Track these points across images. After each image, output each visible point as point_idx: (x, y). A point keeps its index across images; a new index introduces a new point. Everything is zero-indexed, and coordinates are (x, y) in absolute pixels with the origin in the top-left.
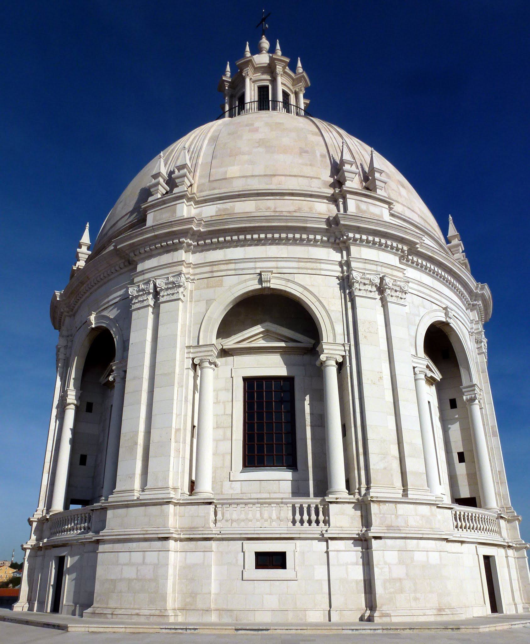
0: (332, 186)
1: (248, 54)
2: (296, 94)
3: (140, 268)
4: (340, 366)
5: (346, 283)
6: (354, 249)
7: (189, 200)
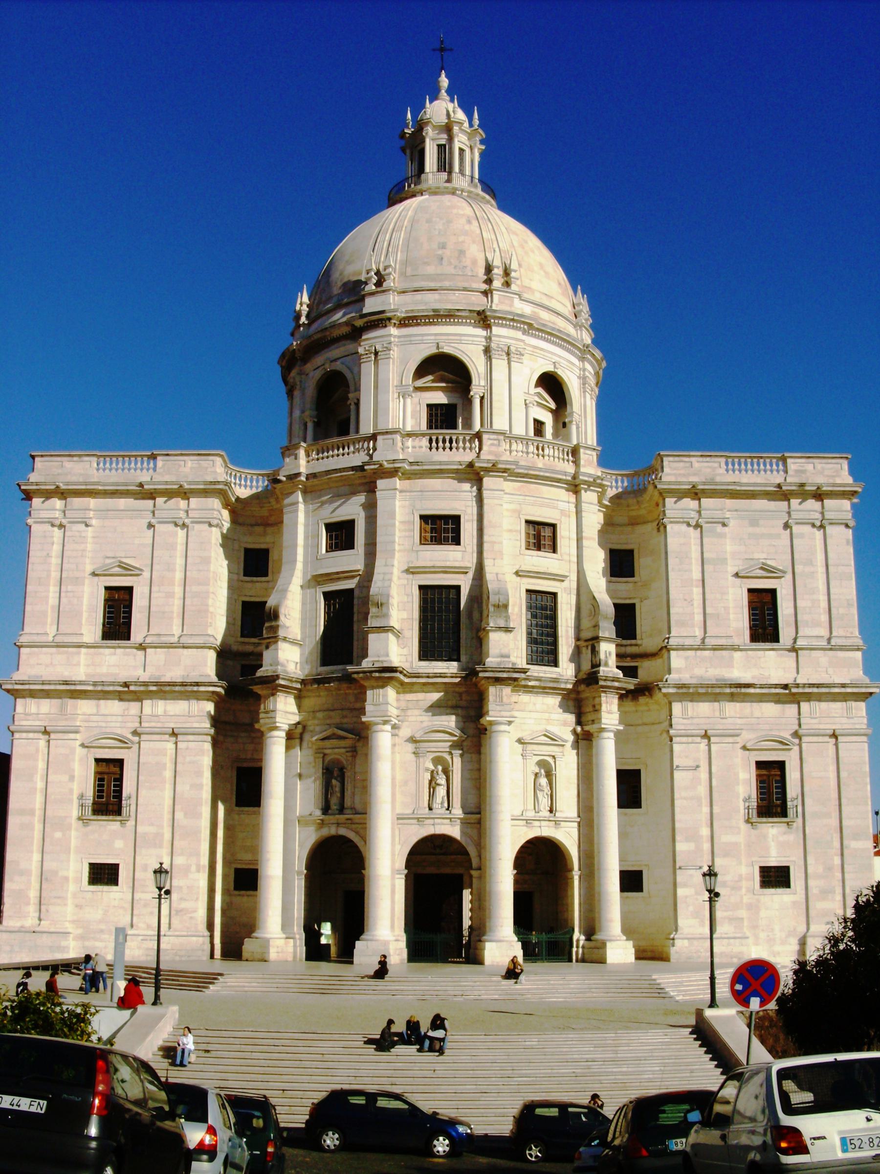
0: (486, 282)
2: (471, 148)
3: (364, 337)
4: (482, 398)
5: (487, 351)
6: (494, 328)
7: (394, 291)
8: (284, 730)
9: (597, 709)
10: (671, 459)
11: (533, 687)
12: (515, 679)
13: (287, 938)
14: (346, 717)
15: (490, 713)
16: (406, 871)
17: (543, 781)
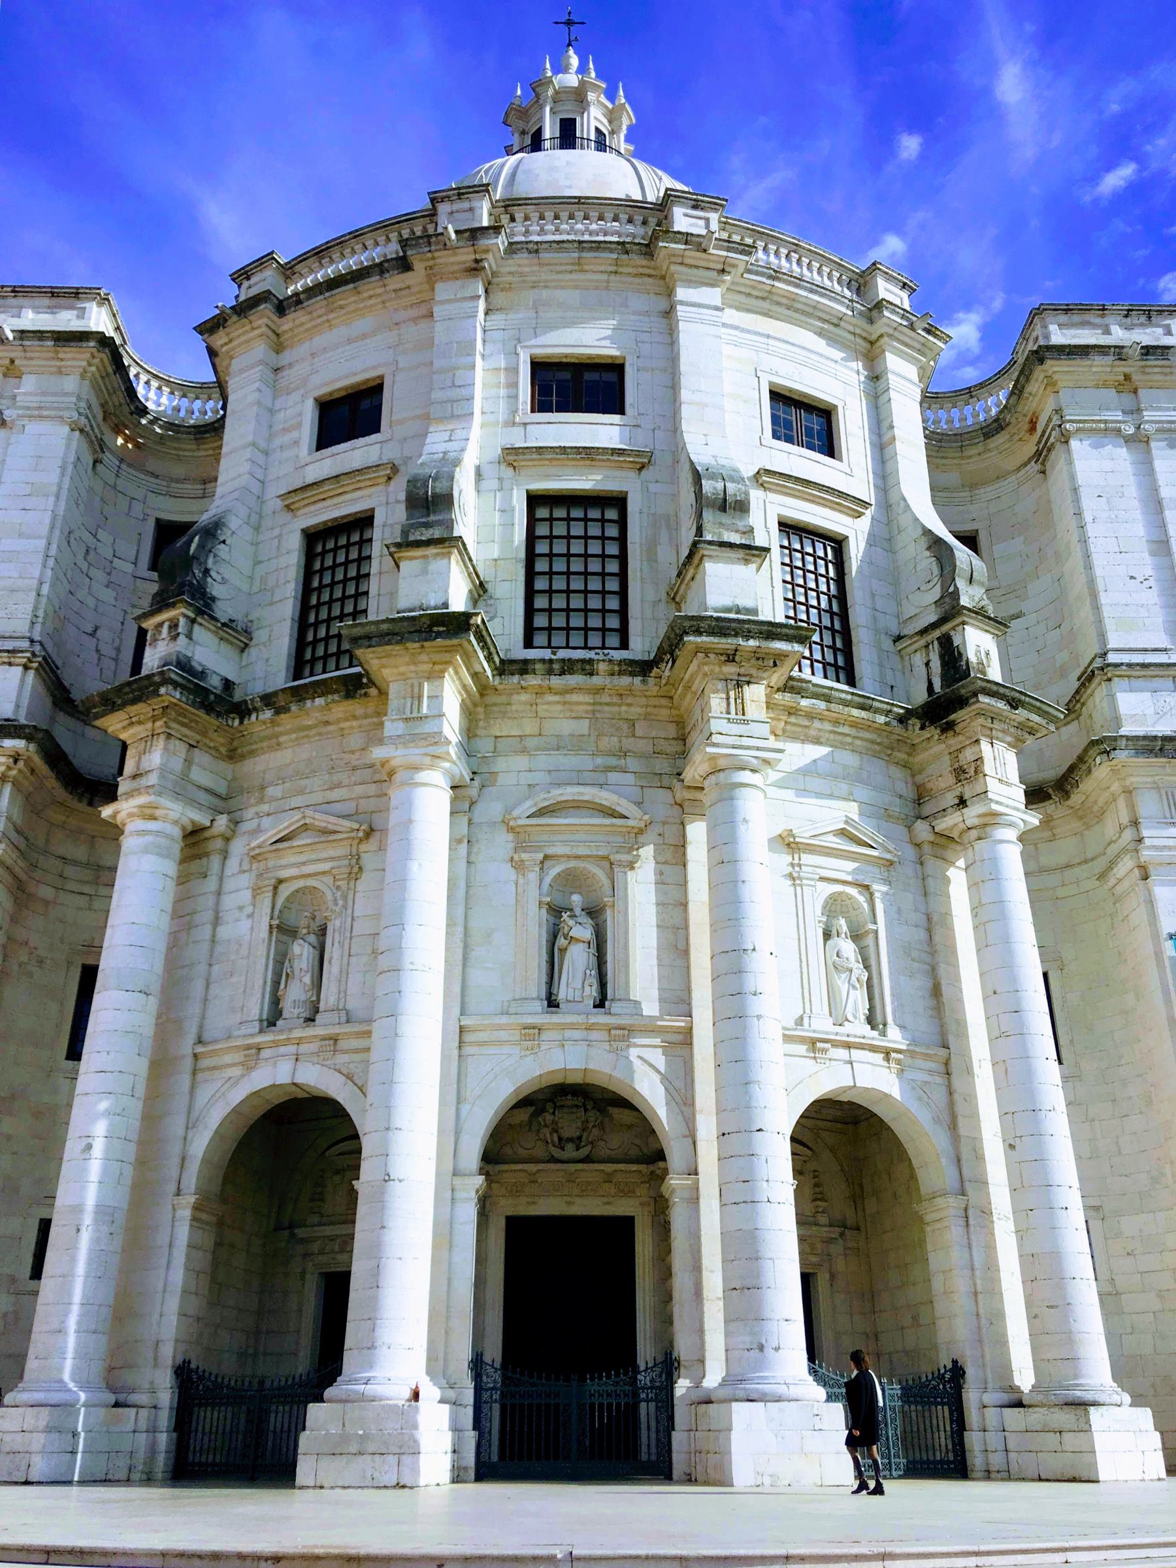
1: (549, 74)
8: (176, 822)
9: (967, 773)
10: (1063, 318)
11: (811, 716)
12: (777, 660)
13: (117, 1405)
14: (339, 785)
15: (716, 739)
16: (480, 1180)
17: (848, 948)
